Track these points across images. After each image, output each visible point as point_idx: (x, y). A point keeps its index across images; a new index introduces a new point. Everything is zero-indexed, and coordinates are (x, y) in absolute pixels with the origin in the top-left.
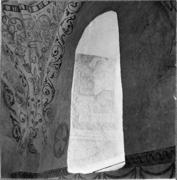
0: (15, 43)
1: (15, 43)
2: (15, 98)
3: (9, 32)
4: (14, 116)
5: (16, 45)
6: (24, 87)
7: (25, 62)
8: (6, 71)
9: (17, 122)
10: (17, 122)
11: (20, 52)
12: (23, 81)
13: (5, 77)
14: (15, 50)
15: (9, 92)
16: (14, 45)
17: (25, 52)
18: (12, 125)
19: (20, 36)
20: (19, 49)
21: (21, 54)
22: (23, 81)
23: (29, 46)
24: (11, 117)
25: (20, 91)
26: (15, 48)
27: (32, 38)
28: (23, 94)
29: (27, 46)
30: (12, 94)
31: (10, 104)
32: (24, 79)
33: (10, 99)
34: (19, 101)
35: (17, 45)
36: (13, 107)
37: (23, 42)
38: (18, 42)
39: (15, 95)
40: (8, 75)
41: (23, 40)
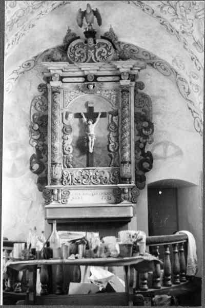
0: (179, 19)
1: (179, 19)
2: (190, 86)
3: (170, 5)
4: (193, 108)
5: (181, 20)
6: (198, 71)
7: (194, 39)
8: (175, 55)
9: (197, 113)
10: (197, 113)
11: (186, 28)
12: (195, 63)
13: (175, 64)
14: (181, 28)
15: (182, 81)
16: (178, 20)
17: (192, 26)
18: (192, 117)
19: (183, 6)
20: (185, 24)
21: (188, 31)
22: (195, 63)
23: (196, 17)
24: (190, 109)
25: (194, 77)
26: (180, 25)
27: (198, 6)
28: (199, 80)
29: (193, 17)
30: (186, 82)
31: (186, 94)
32: (197, 61)
33: (184, 88)
34: (196, 89)
35: (182, 19)
36: (189, 97)
37: (188, 14)
38: (182, 16)
39: (189, 84)
40: (178, 61)
41: (188, 11)
